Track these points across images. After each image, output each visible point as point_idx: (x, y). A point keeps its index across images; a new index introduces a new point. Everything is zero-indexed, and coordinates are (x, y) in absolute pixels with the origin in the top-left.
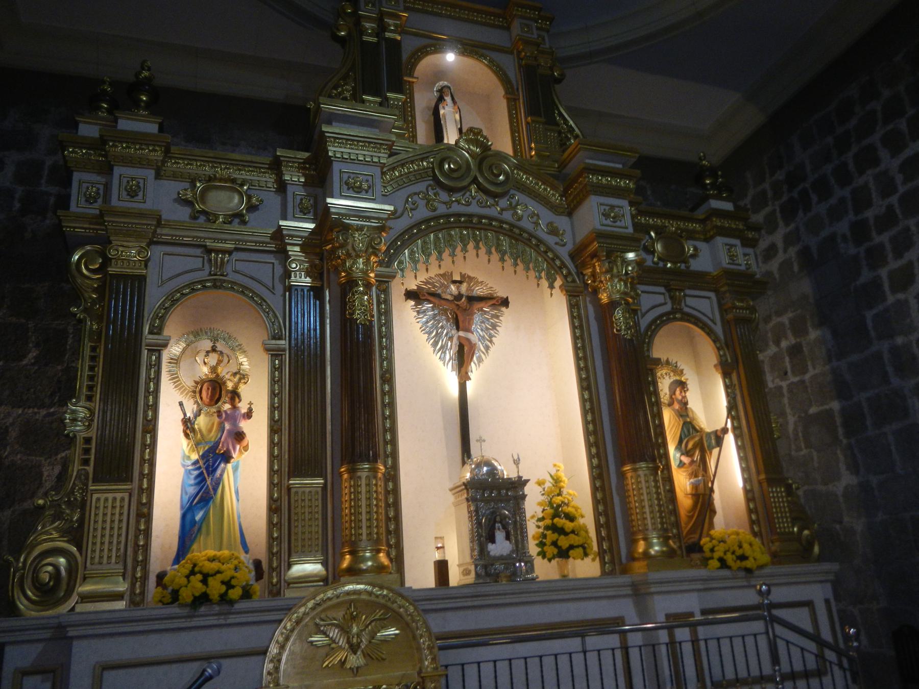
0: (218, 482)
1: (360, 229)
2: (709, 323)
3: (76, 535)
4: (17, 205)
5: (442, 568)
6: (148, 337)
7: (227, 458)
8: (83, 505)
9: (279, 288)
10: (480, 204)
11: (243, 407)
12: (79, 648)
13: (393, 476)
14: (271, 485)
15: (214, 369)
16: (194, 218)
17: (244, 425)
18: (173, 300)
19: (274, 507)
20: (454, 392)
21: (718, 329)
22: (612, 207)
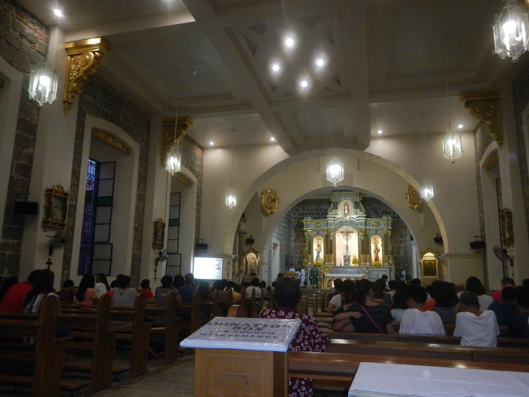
0: (319, 255)
1: (331, 230)
2: (381, 235)
3: (307, 259)
4: (298, 219)
5: (341, 264)
6: (312, 241)
7: (320, 252)
8: (308, 257)
9: (324, 234)
10: (347, 222)
11: (321, 247)
12: (308, 269)
13: (335, 255)
14: (324, 255)
15: (318, 243)
16: (315, 227)
17: (321, 249)
18: (314, 237)
19: (324, 257)
20: (346, 245)
21: (383, 235)
22: (362, 223)
